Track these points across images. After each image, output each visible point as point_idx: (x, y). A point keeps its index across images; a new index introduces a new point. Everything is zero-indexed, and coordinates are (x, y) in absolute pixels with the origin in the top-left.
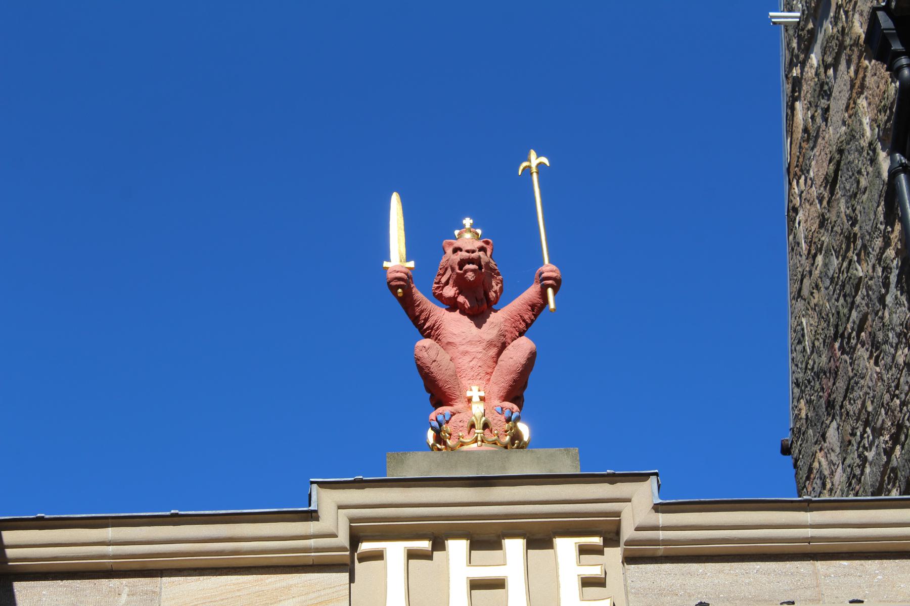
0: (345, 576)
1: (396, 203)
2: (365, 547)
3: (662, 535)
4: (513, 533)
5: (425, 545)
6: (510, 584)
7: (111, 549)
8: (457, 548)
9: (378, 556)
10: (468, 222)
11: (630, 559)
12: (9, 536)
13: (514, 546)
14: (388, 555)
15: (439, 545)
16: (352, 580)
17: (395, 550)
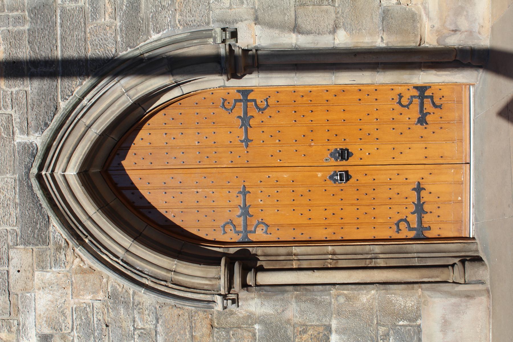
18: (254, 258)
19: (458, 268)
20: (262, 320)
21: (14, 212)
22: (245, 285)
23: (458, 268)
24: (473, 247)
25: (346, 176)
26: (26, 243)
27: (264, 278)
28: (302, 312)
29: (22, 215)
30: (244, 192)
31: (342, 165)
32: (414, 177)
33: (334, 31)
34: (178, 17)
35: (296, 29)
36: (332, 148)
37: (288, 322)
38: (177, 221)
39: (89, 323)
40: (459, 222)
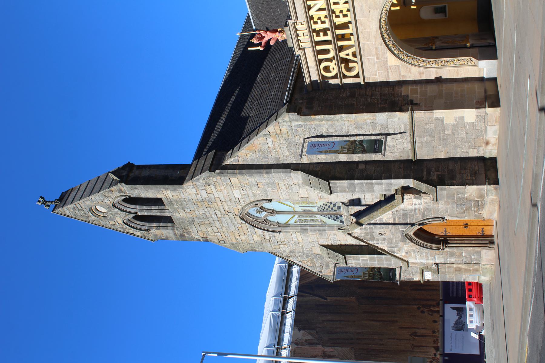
0: (305, 49)
1: (249, 49)
2: (301, 47)
3: (295, 18)
4: (296, 32)
5: (299, 41)
6: (303, 32)
7: (307, 73)
8: (299, 38)
9: (302, 46)
10: (251, 41)
11: (298, 20)
12: (307, 83)
13: (298, 32)
14: (301, 45)
15: (299, 40)
16: (305, 48)
17: (301, 44)
18: (447, 240)
19: (489, 244)
20: (449, 251)
21: (400, 238)
22: (446, 247)
23: (489, 244)
24: (493, 238)
25: (467, 227)
26: (402, 242)
27: (449, 245)
28: (457, 250)
29: (401, 238)
30: (445, 229)
31: (465, 226)
32: (482, 227)
33: (465, 217)
34: (433, 215)
35: (457, 217)
36: (464, 223)
37: (454, 252)
38: (431, 232)
39: (415, 251)
40: (491, 233)
